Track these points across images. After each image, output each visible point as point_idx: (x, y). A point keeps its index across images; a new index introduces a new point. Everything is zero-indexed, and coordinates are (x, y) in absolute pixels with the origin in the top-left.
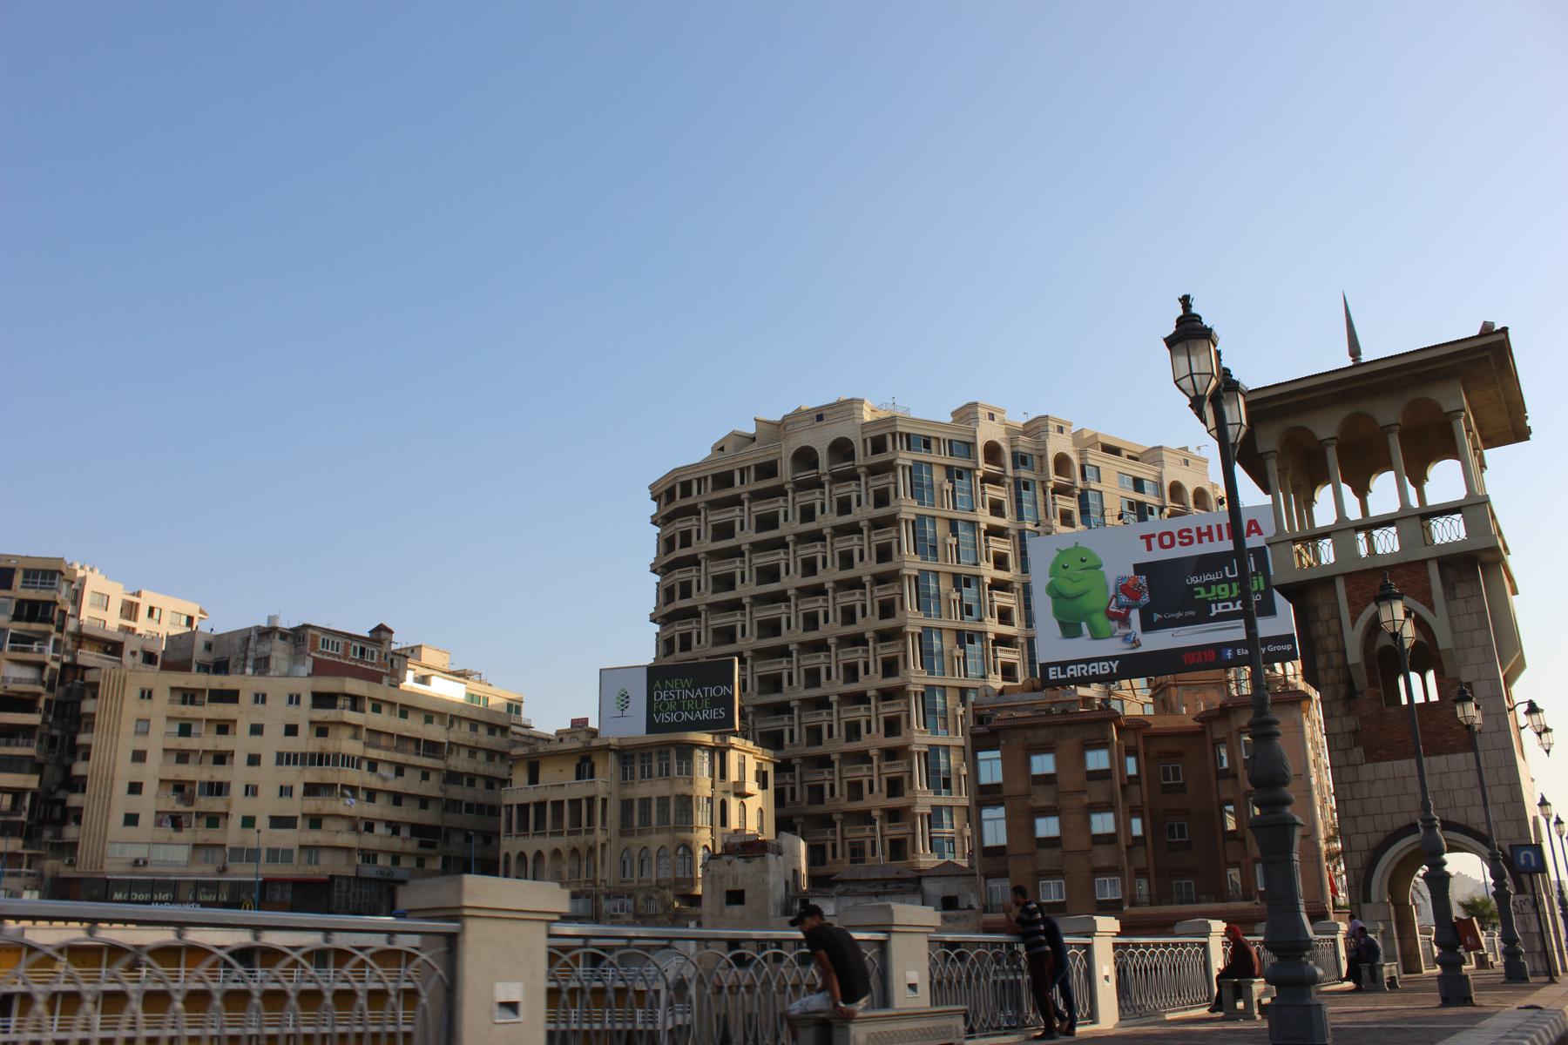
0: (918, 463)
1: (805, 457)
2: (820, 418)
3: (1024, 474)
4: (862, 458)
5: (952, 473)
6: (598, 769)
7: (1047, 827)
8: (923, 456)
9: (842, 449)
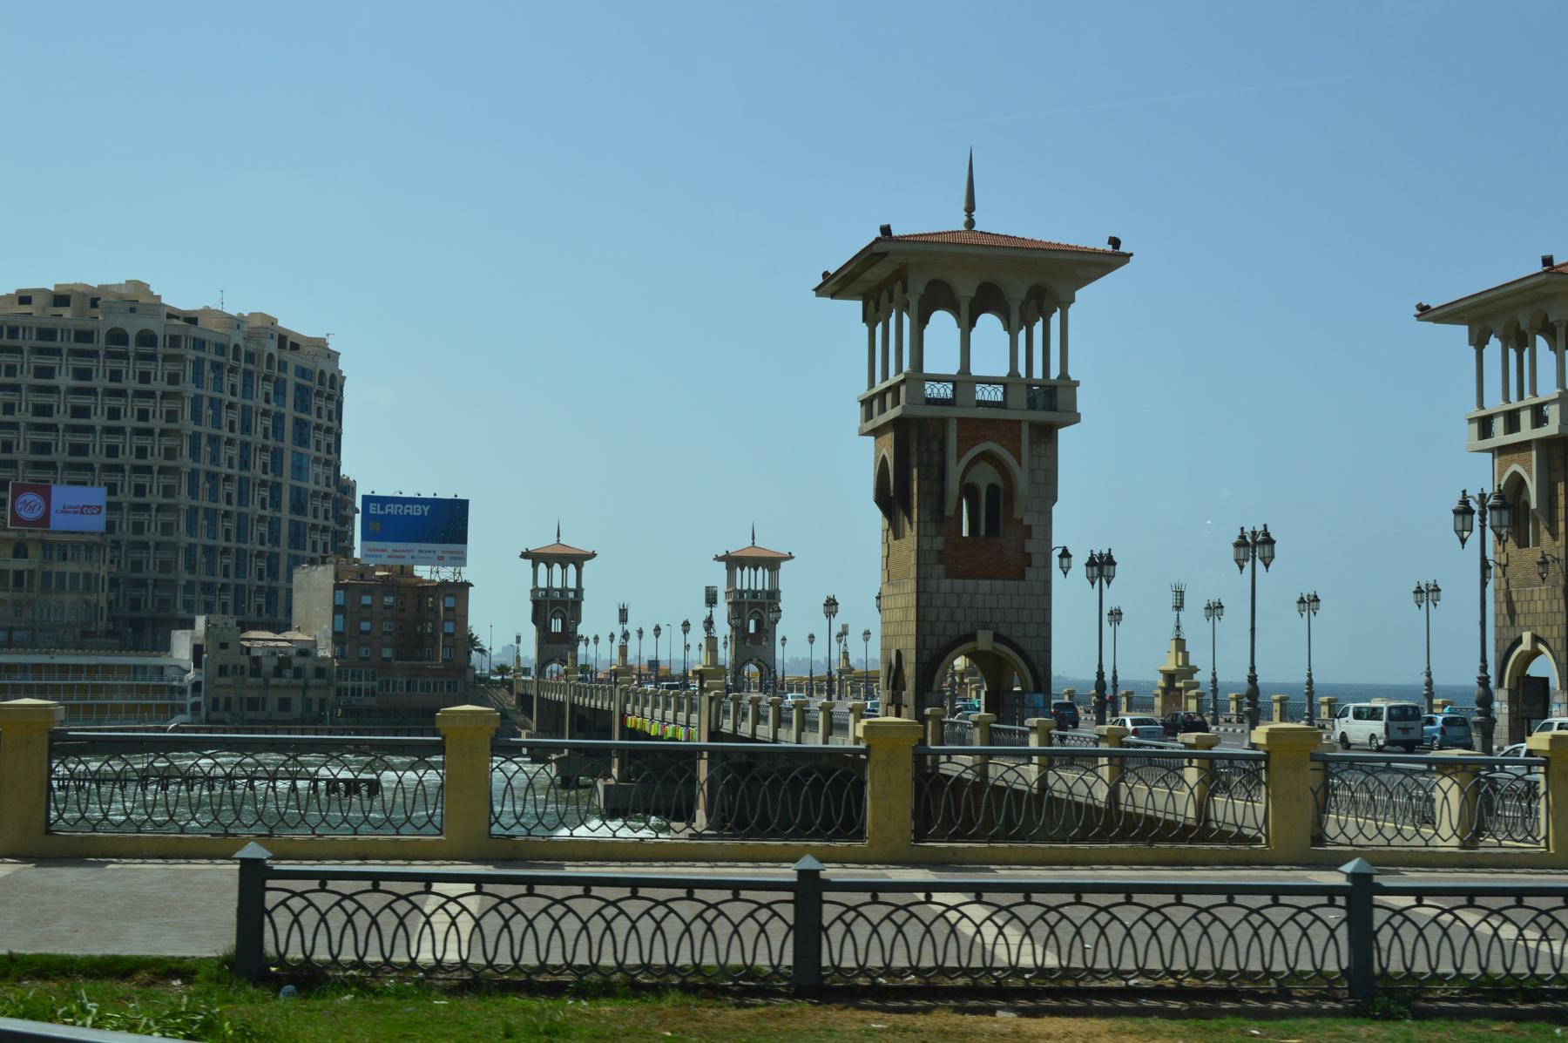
0: (198, 359)
1: (118, 336)
2: (132, 310)
3: (251, 367)
4: (161, 349)
5: (216, 367)
6: (31, 552)
7: (365, 626)
8: (201, 354)
9: (147, 338)
